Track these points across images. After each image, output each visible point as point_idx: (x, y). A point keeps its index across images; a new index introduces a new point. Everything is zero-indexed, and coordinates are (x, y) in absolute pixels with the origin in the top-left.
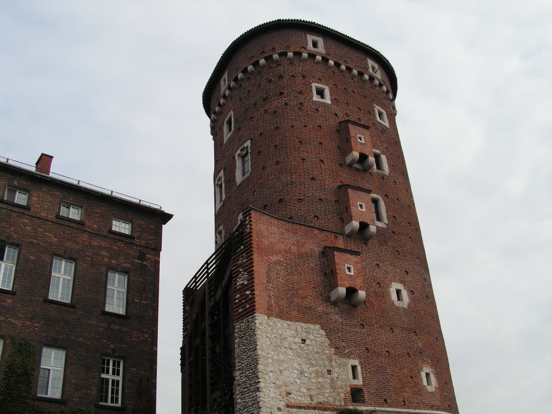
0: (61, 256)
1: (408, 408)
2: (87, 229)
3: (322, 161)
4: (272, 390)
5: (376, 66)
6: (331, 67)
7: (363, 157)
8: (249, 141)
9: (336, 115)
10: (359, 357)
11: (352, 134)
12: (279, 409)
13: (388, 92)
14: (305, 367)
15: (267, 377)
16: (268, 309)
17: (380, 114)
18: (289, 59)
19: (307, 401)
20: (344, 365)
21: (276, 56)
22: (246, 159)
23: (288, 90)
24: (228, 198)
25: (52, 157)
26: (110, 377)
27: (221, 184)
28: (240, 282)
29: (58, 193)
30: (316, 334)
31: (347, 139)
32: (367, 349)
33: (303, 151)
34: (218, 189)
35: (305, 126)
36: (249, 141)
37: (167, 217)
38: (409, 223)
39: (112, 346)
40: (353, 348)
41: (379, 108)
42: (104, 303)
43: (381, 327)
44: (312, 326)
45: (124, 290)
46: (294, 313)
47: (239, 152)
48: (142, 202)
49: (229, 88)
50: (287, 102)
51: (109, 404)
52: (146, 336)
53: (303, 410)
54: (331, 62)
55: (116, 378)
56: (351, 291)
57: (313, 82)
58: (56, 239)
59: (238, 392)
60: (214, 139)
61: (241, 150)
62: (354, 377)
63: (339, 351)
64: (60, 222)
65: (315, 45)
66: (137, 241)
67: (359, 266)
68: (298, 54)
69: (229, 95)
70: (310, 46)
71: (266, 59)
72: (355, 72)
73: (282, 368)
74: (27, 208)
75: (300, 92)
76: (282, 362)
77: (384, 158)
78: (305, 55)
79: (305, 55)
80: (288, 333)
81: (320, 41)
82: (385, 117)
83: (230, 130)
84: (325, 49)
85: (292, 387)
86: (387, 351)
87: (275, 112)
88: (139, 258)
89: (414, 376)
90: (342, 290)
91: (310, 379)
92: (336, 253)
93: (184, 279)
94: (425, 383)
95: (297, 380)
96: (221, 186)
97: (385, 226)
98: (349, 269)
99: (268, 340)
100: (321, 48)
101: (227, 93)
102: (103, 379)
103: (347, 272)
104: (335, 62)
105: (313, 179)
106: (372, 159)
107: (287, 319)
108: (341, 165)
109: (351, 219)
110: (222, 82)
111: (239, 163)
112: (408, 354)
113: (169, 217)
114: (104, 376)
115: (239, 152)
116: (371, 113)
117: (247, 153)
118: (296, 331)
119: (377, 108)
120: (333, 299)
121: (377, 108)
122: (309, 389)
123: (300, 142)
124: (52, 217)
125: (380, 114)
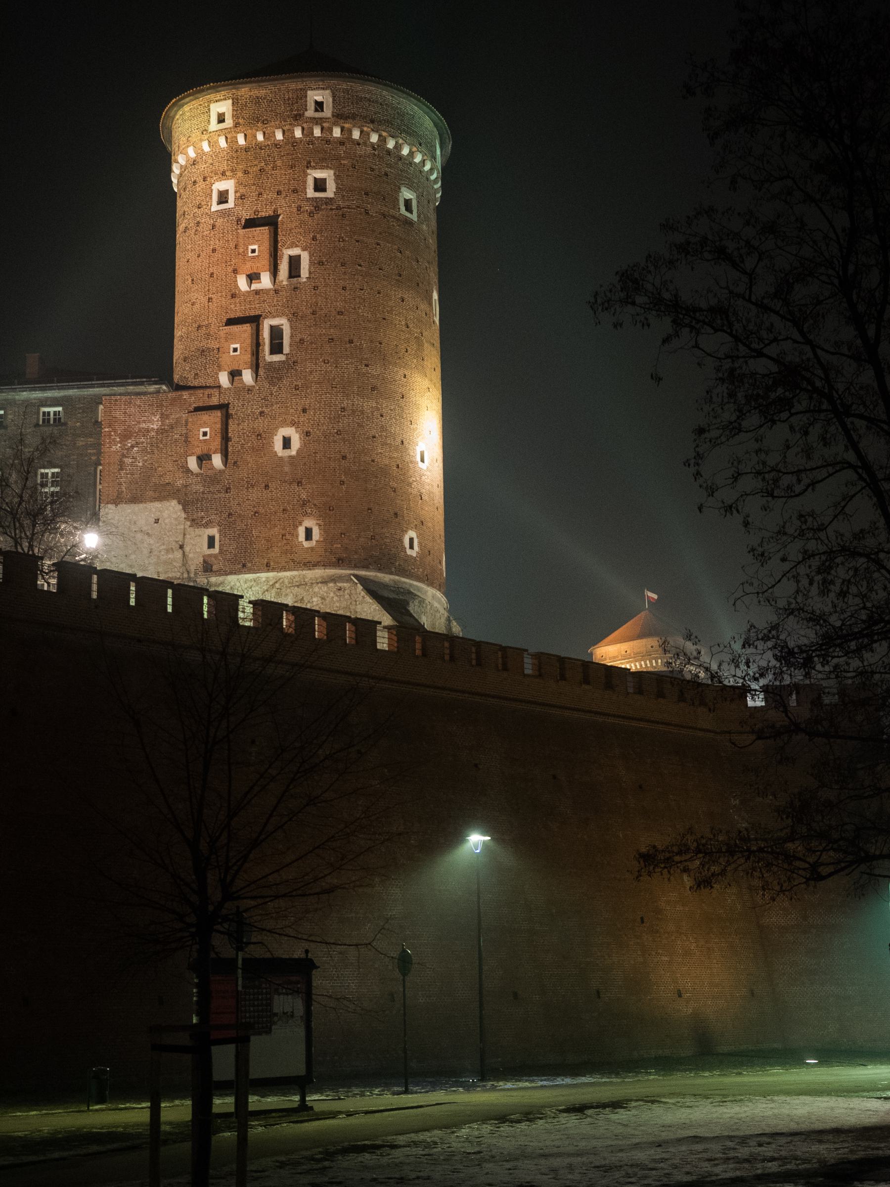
32: (230, 514)
43: (253, 486)
62: (211, 544)
63: (195, 523)
103: (201, 438)
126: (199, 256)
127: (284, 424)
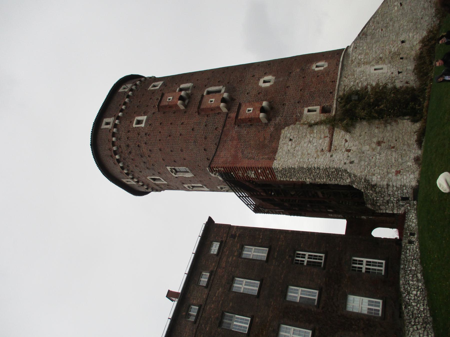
0: (231, 286)
1: (337, 79)
2: (215, 270)
3: (182, 123)
4: (319, 160)
5: (124, 86)
6: (123, 115)
7: (181, 98)
8: (167, 167)
9: (154, 113)
10: (303, 107)
11: (167, 104)
12: (331, 156)
13: (140, 81)
14: (306, 140)
15: (311, 163)
16: (270, 159)
17: (154, 86)
18: (117, 140)
19: (327, 140)
20: (307, 116)
21: (115, 148)
22: (178, 170)
23: (136, 142)
24: (201, 182)
25: (169, 290)
26: (306, 260)
27: (192, 186)
28: (253, 176)
29: (192, 287)
30: (287, 132)
31: (170, 107)
32: (298, 102)
33: (175, 134)
34: (195, 188)
35: (160, 132)
36: (167, 167)
37: (210, 220)
38: (223, 73)
39: (287, 258)
40: (297, 111)
41: (151, 86)
42: (261, 261)
43: (286, 93)
44: (282, 135)
45: (254, 248)
46: (273, 144)
47: (173, 174)
48: (200, 235)
49: (132, 179)
50: (144, 142)
51: (323, 261)
52: (282, 236)
53: (333, 142)
54: (120, 114)
55: (307, 256)
56: (263, 110)
57: (132, 126)
58: (220, 289)
59: (319, 180)
60: (164, 190)
61: (172, 173)
62: (315, 111)
64: (210, 286)
65: (107, 124)
66: (224, 239)
67: (247, 104)
68: (114, 135)
69: (137, 179)
70: (108, 126)
71: (116, 154)
72: (127, 100)
73: (306, 153)
74: (200, 306)
75: (138, 134)
76: (302, 153)
77: (182, 86)
78: (115, 130)
79: (115, 130)
80: (285, 148)
81: (106, 120)
82: (156, 84)
83: (159, 179)
84: (111, 117)
85: (318, 148)
86: (301, 90)
87: (150, 150)
88: (234, 238)
89: (317, 75)
90: (262, 115)
91: (314, 137)
92: (239, 118)
93: (249, 212)
94: (322, 68)
95: (314, 145)
96: (193, 187)
97: (224, 88)
98: (249, 111)
99: (289, 161)
100: (111, 120)
101: (136, 180)
102: (307, 264)
103: (251, 112)
104: (120, 112)
105: (193, 129)
106: (183, 93)
107: (277, 149)
108: (185, 112)
109: (219, 108)
110: (129, 183)
111: (180, 175)
112: (303, 78)
113: (210, 219)
114: (305, 263)
115: (173, 174)
116: (153, 92)
117: (174, 169)
118: (284, 144)
119: (151, 88)
120: (267, 122)
121: (151, 88)
122: (320, 138)
123: (170, 136)
124: (206, 291)
125: (154, 86)
126: (160, 132)
127: (257, 83)
